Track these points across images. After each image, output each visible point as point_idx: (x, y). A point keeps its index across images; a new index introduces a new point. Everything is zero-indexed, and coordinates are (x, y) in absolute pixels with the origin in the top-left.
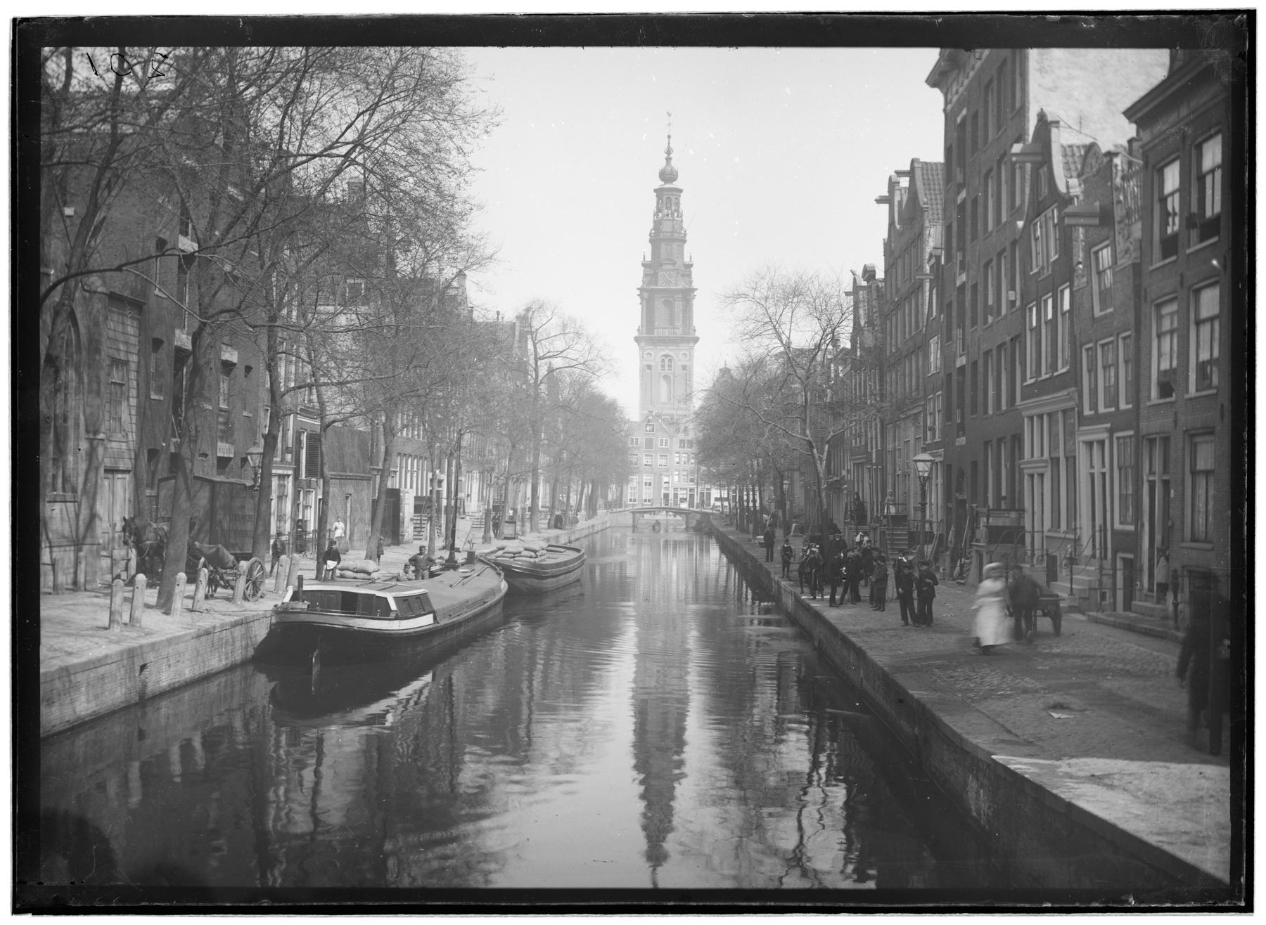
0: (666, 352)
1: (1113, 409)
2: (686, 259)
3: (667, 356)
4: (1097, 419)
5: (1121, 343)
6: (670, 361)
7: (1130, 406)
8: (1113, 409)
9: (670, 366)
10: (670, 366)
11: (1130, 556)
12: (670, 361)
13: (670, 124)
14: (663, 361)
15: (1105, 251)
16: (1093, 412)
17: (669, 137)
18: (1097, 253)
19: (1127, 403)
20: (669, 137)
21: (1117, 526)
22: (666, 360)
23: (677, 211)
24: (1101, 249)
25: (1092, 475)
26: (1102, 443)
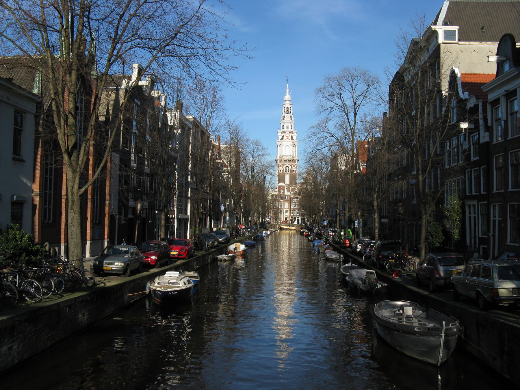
0: (287, 165)
1: (478, 194)
4: (472, 197)
5: (481, 170)
7: (485, 193)
8: (478, 194)
9: (288, 170)
10: (288, 170)
11: (486, 246)
13: (288, 80)
15: (475, 136)
16: (470, 194)
18: (473, 137)
19: (484, 191)
21: (480, 236)
22: (287, 168)
23: (290, 112)
24: (474, 135)
25: (470, 217)
26: (474, 206)
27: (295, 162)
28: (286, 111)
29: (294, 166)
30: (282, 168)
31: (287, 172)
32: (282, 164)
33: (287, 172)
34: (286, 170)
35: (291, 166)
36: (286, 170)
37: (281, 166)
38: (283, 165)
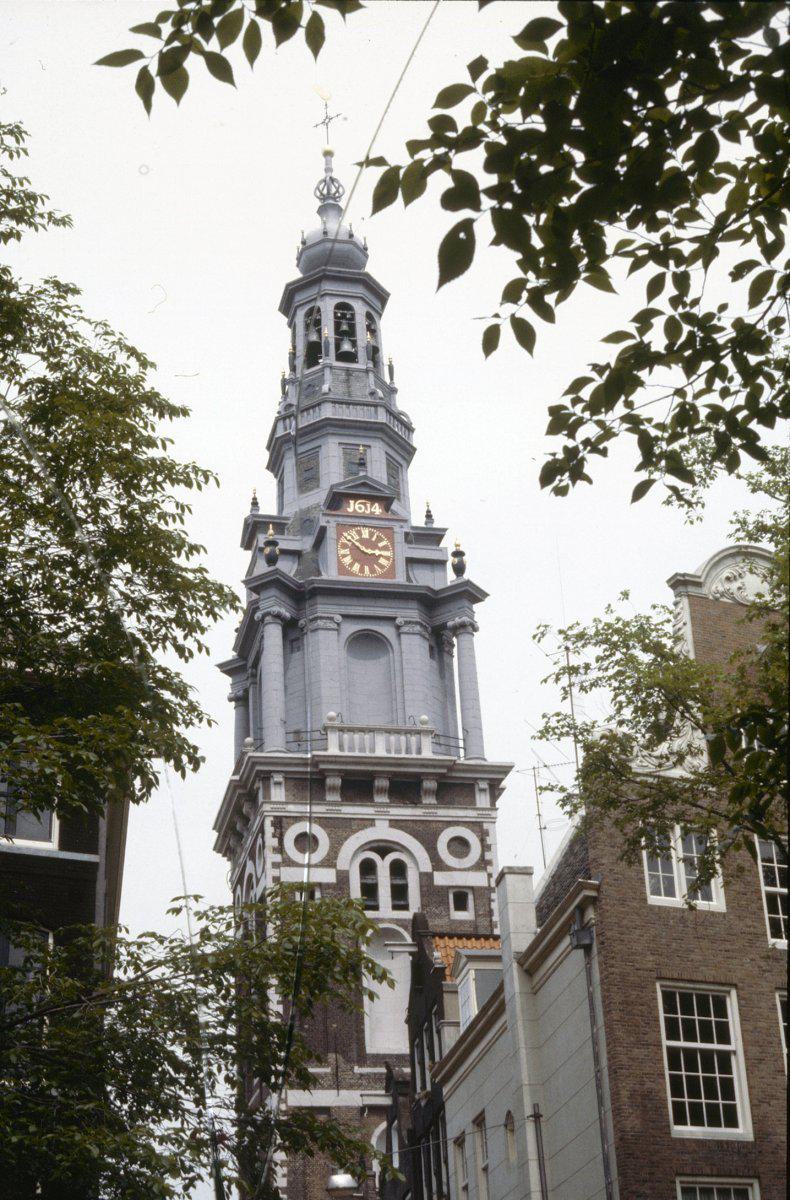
0: (382, 831)
2: (418, 520)
3: (383, 848)
6: (398, 869)
9: (399, 894)
10: (399, 894)
12: (398, 869)
14: (368, 868)
17: (328, 154)
20: (328, 154)
22: (383, 867)
23: (374, 352)
27: (471, 803)
28: (328, 331)
29: (460, 846)
30: (329, 862)
31: (385, 909)
32: (324, 822)
33: (385, 909)
34: (370, 891)
35: (428, 839)
36: (370, 891)
37: (306, 842)
38: (340, 829)
